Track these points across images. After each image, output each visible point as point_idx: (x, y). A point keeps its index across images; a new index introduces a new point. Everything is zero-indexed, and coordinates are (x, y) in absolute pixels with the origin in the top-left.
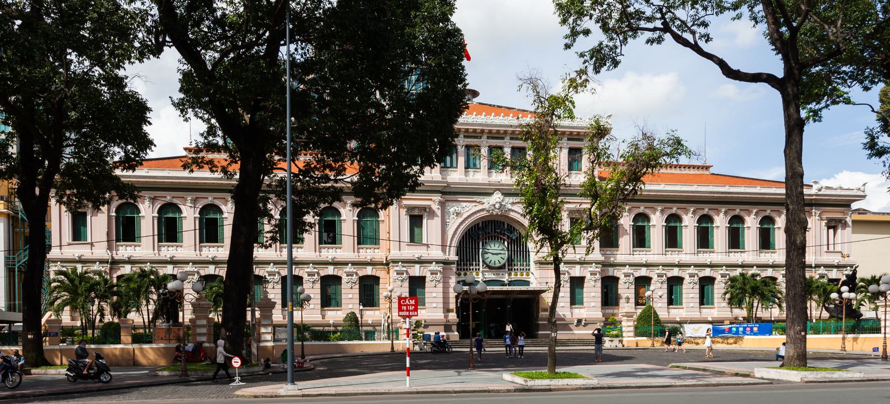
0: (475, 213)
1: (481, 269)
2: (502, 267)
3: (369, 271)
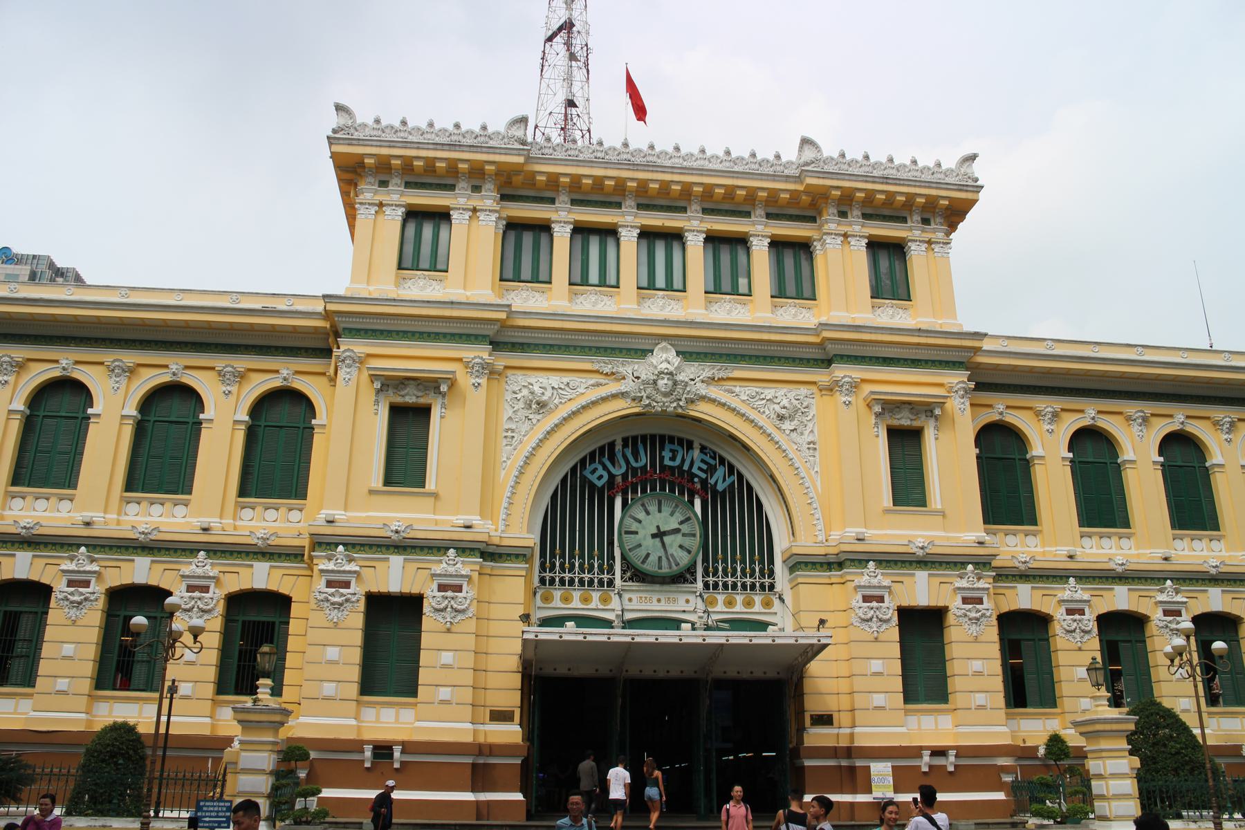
0: (594, 403)
1: (618, 582)
3: (260, 576)
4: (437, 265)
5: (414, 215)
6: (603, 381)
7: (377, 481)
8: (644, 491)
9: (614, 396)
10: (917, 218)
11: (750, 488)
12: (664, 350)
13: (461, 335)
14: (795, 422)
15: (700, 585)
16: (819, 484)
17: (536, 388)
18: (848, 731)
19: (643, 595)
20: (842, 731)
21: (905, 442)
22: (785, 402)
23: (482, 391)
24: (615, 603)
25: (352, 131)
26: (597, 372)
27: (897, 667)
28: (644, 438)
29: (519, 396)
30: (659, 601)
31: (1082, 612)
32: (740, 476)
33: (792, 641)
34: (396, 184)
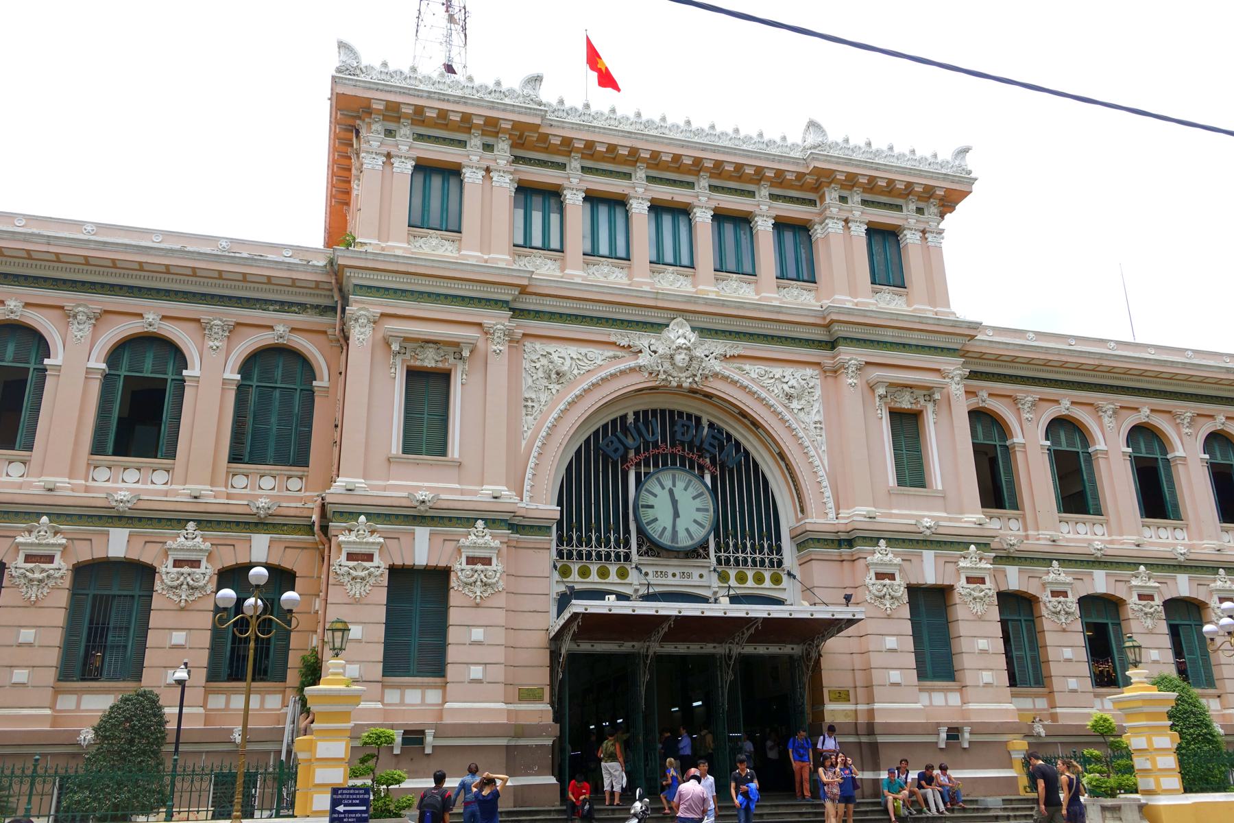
1: (634, 556)
2: (696, 552)
4: (451, 226)
5: (423, 168)
6: (619, 354)
7: (396, 447)
8: (656, 465)
9: (632, 370)
10: (912, 207)
11: (756, 465)
12: (682, 326)
13: (480, 300)
14: (803, 402)
15: (713, 560)
16: (826, 463)
17: (555, 357)
18: (865, 707)
19: (659, 569)
20: (860, 707)
21: (906, 425)
22: (793, 382)
23: (504, 359)
24: (634, 577)
25: (358, 72)
26: (614, 344)
27: (909, 643)
28: (654, 412)
29: (538, 365)
30: (674, 575)
31: (1065, 594)
32: (747, 453)
33: (808, 616)
34: (405, 131)
